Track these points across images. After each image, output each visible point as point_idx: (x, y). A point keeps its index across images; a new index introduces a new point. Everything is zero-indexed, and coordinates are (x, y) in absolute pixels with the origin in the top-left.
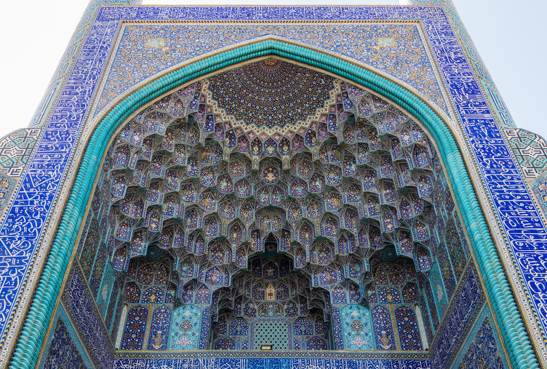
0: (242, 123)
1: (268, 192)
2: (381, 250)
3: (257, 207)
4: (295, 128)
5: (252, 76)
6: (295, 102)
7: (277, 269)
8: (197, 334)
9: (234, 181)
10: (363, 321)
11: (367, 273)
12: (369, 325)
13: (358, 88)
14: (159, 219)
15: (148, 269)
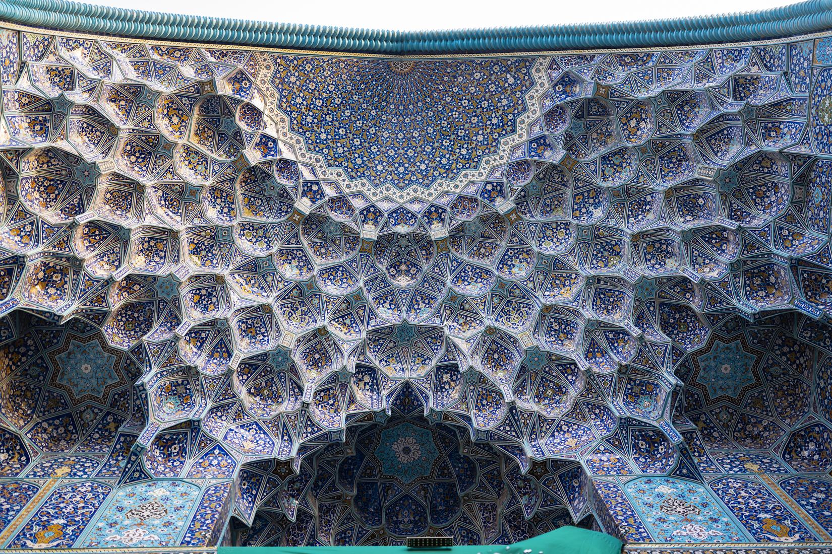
0: (339, 174)
1: (397, 307)
2: (700, 352)
3: (373, 323)
4: (456, 187)
5: (363, 86)
6: (453, 137)
7: (422, 514)
8: (180, 523)
9: (317, 269)
10: (694, 499)
11: (675, 393)
12: (716, 507)
13: (582, 58)
14: (117, 267)
15: (66, 427)
